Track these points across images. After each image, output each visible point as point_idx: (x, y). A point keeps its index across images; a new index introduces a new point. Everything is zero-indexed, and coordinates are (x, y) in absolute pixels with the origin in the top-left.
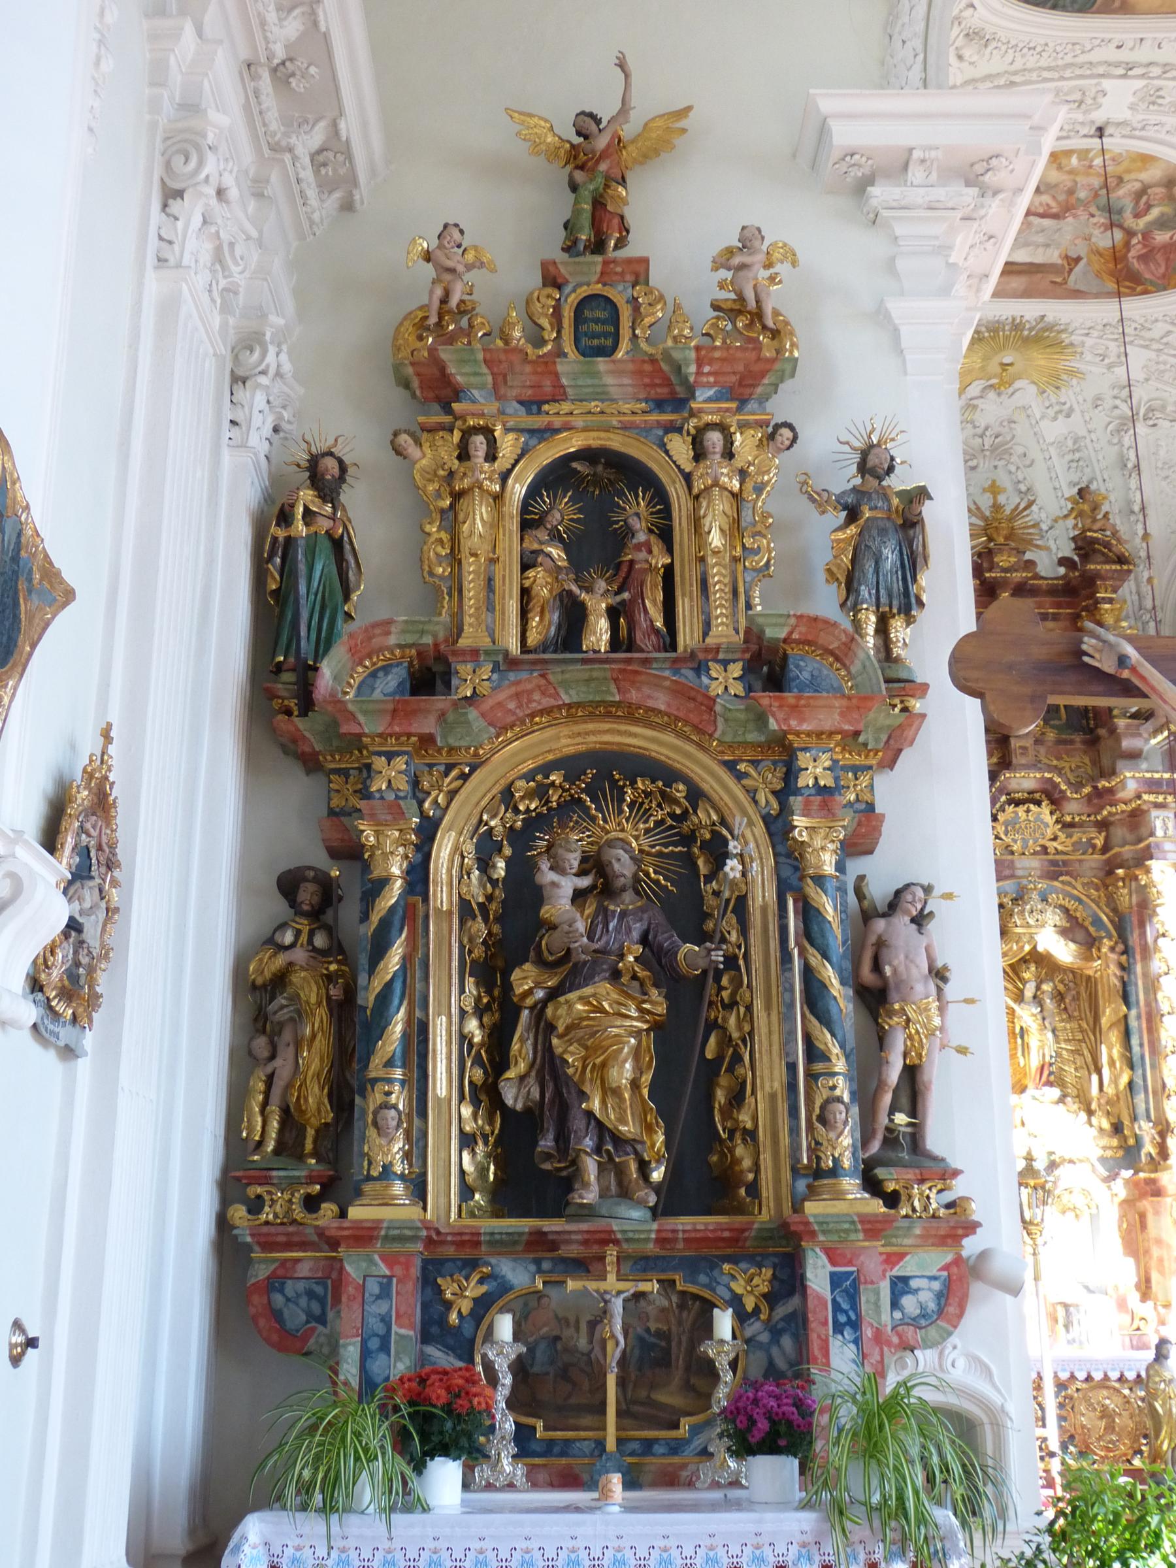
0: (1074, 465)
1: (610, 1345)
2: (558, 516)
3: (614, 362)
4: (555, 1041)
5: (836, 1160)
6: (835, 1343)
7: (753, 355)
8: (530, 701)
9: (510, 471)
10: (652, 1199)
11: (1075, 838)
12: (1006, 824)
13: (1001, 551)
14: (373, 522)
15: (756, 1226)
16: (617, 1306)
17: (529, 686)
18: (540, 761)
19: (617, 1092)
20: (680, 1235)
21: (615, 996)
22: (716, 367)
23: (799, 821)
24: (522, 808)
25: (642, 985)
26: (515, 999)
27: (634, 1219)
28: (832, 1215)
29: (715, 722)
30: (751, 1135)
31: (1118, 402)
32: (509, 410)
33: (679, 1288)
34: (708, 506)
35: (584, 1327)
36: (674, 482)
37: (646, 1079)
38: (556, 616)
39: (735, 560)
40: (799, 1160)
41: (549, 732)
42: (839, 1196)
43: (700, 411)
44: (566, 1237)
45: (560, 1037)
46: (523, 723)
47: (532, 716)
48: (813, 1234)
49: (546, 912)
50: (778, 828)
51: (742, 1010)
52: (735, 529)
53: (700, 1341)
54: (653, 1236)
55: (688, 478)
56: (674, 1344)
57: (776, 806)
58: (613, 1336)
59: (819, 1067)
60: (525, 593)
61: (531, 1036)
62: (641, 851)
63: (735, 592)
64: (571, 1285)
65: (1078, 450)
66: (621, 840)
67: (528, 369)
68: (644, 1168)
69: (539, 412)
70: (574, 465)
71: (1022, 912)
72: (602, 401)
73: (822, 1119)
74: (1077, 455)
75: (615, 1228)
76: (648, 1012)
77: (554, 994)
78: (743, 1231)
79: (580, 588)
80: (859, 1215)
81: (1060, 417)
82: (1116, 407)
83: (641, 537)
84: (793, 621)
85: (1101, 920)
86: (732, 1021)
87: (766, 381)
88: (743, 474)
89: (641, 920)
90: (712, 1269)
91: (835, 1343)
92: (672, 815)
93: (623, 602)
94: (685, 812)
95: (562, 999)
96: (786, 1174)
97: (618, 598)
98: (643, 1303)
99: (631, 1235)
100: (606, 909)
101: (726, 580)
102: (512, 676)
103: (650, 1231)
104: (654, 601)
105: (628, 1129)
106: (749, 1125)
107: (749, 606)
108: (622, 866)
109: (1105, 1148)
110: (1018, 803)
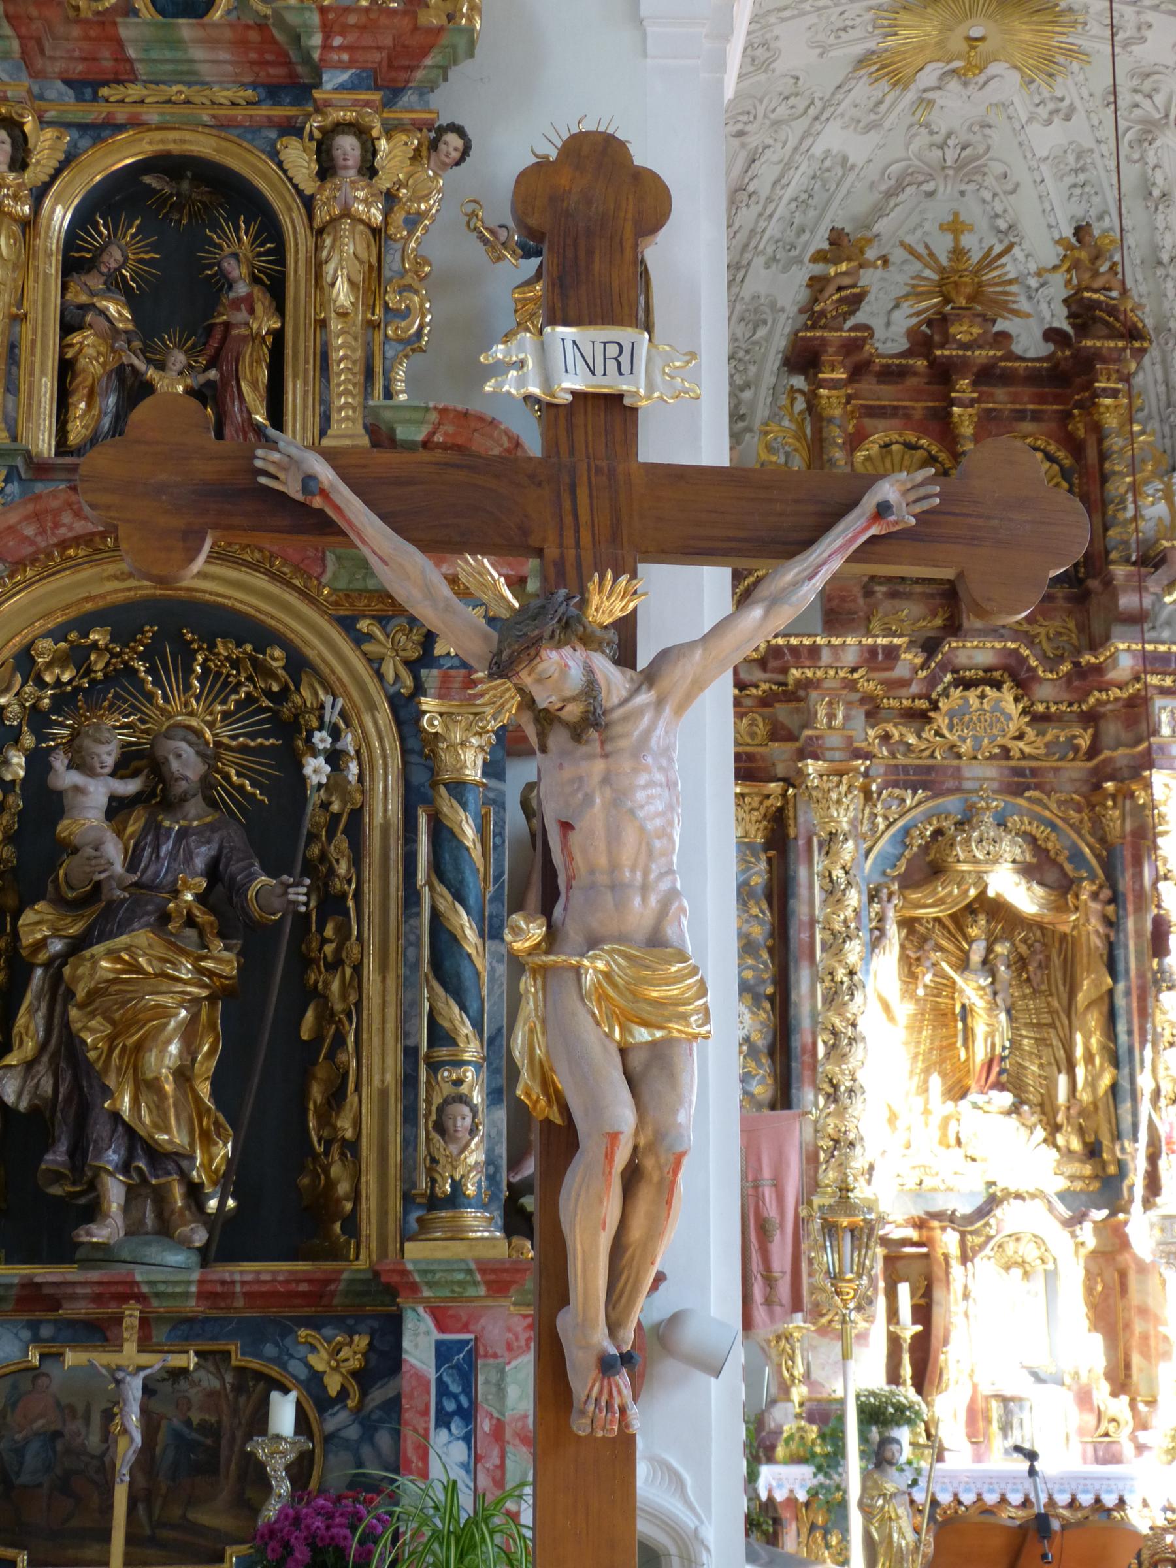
0: (1078, 191)
1: (122, 1443)
2: (117, 254)
3: (203, 26)
4: (74, 1013)
5: (457, 1185)
6: (439, 1438)
7: (406, 23)
8: (57, 525)
9: (45, 187)
10: (200, 1237)
11: (1049, 737)
12: (951, 714)
13: (959, 318)
15: (345, 1276)
16: (134, 1388)
17: (55, 504)
18: (73, 613)
19: (154, 1086)
20: (238, 1288)
21: (160, 951)
22: (351, 38)
23: (429, 704)
24: (48, 678)
25: (201, 935)
26: (24, 953)
27: (172, 1266)
28: (440, 1261)
29: (323, 559)
30: (352, 1147)
31: (1138, 98)
32: (51, 94)
33: (234, 1362)
34: (332, 247)
35: (96, 1418)
36: (290, 209)
37: (206, 1066)
38: (112, 400)
39: (372, 326)
40: (414, 1185)
41: (87, 573)
42: (457, 1234)
43: (328, 104)
44: (69, 1290)
45: (81, 1006)
46: (49, 556)
47: (63, 545)
48: (414, 1288)
49: (64, 828)
50: (405, 712)
51: (348, 971)
52: (374, 279)
53: (249, 1437)
54: (194, 1289)
55: (308, 203)
56: (224, 1442)
57: (409, 682)
58: (125, 1431)
59: (443, 1053)
60: (66, 369)
61: (44, 1006)
62: (218, 744)
63: (369, 374)
64: (72, 1358)
65: (1083, 169)
66: (189, 728)
67: (76, 31)
68: (195, 1193)
69: (95, 98)
70: (147, 179)
71: (968, 841)
72: (189, 84)
73: (441, 1128)
74: (1082, 177)
75: (138, 1278)
76: (210, 973)
77: (77, 946)
78: (328, 1282)
79: (149, 361)
80: (478, 1261)
81: (1057, 120)
82: (1137, 106)
83: (242, 289)
84: (434, 416)
85: (1082, 853)
86: (335, 986)
87: (428, 62)
88: (390, 199)
89: (208, 842)
90: (283, 1336)
91: (439, 1438)
92: (268, 694)
93: (210, 383)
94: (285, 689)
95: (87, 953)
96: (396, 1204)
97: (202, 379)
98: (183, 1384)
99: (162, 1288)
100: (159, 826)
101: (358, 354)
102: (39, 487)
103: (189, 1282)
104: (254, 384)
105: (174, 1137)
106: (349, 1134)
107: (388, 394)
108: (186, 764)
109: (1072, 1178)
110: (968, 684)
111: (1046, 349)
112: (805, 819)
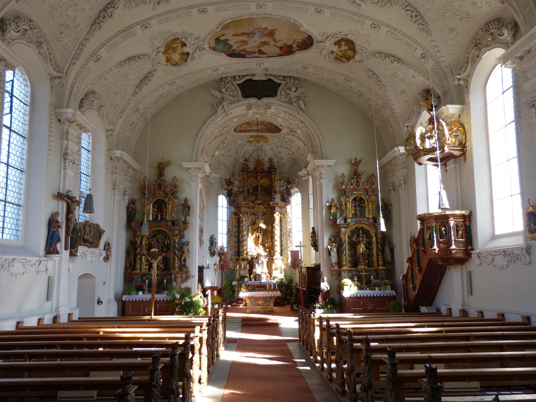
14: (138, 206)
112: (241, 220)
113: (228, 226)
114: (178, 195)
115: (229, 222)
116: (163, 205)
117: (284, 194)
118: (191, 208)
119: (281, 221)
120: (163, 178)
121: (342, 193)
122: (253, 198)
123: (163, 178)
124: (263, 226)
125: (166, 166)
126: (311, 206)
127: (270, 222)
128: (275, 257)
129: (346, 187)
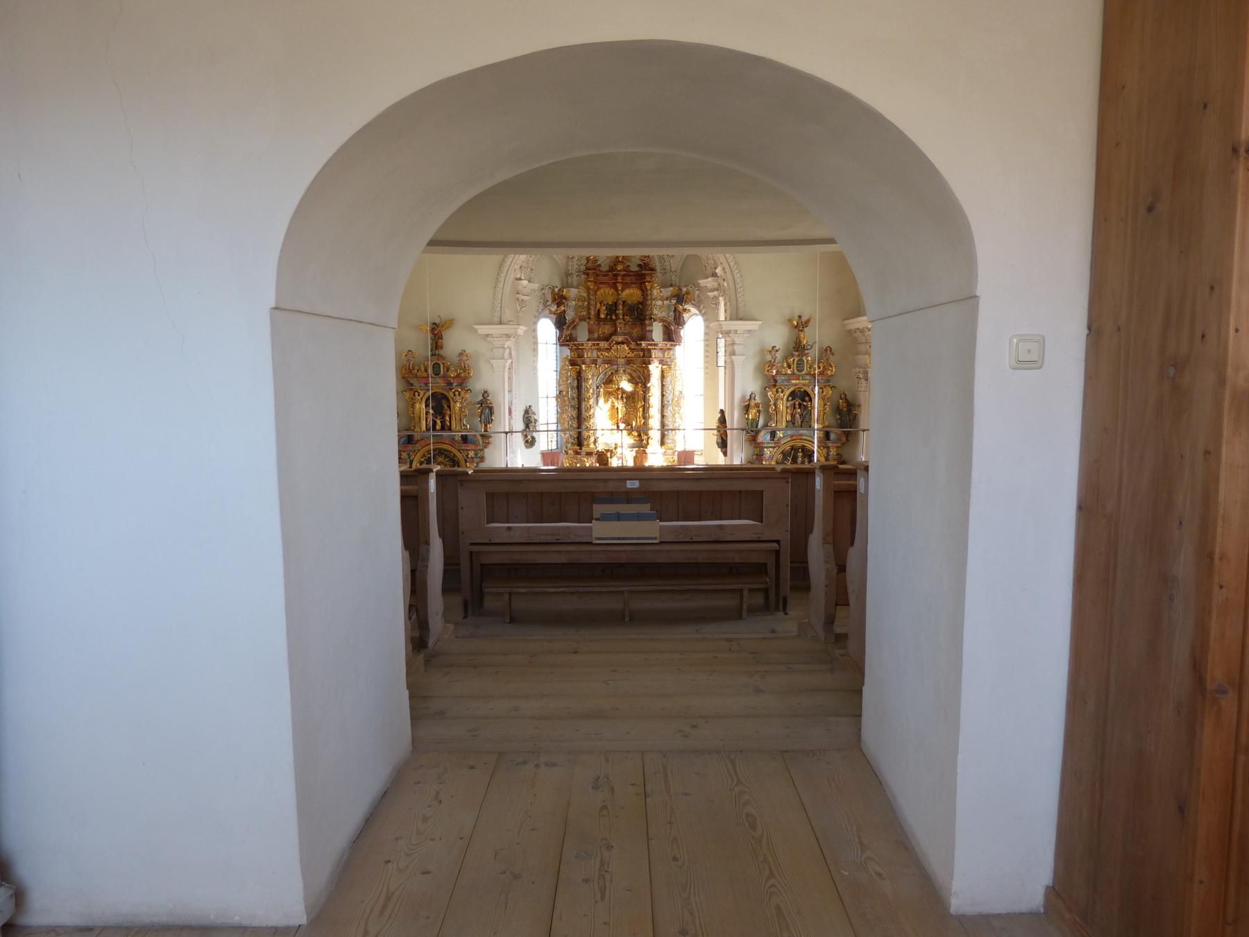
111: (637, 269)
113: (559, 384)
114: (470, 384)
115: (561, 374)
116: (444, 402)
117: (669, 323)
118: (496, 410)
119: (663, 377)
120: (441, 352)
121: (772, 383)
122: (607, 329)
123: (441, 352)
124: (627, 386)
125: (449, 327)
126: (721, 362)
127: (641, 380)
128: (649, 450)
129: (778, 372)
